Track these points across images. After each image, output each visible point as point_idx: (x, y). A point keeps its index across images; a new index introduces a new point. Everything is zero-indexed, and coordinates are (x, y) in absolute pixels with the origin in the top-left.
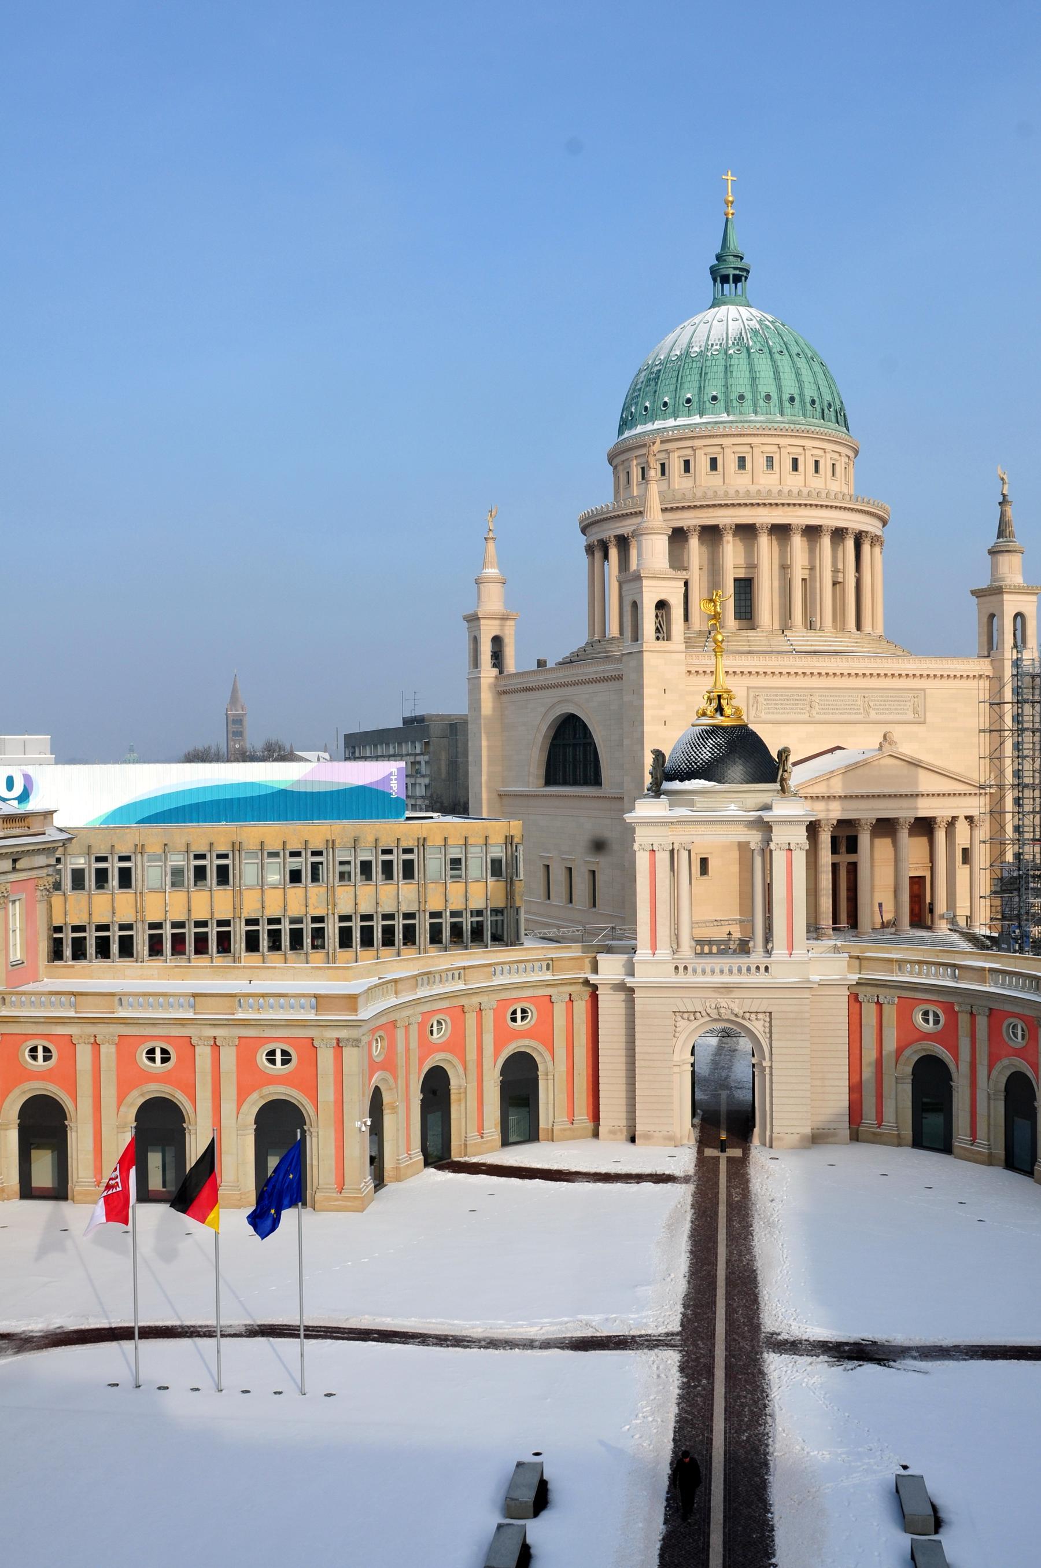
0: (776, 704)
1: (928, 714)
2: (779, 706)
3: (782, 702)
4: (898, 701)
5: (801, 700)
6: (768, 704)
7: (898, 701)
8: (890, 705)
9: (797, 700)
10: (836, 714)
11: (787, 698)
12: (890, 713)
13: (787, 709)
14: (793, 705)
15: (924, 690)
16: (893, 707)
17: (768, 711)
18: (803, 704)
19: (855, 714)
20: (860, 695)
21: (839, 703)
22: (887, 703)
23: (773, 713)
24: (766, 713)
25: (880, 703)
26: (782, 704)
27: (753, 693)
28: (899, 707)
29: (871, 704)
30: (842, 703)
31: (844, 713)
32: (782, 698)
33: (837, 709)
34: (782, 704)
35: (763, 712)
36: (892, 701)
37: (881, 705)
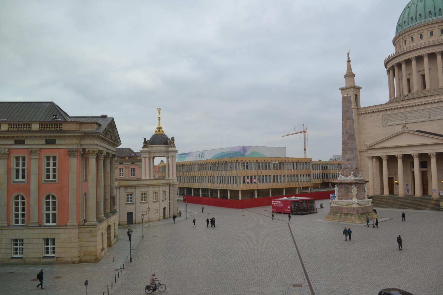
2: (394, 119)
5: (402, 116)
6: (390, 119)
13: (397, 120)
14: (399, 118)
18: (403, 118)
19: (424, 118)
20: (426, 111)
23: (392, 122)
25: (435, 112)
26: (395, 119)
27: (384, 117)
29: (431, 114)
32: (395, 117)
33: (417, 117)
35: (388, 122)
36: (440, 111)
37: (436, 113)
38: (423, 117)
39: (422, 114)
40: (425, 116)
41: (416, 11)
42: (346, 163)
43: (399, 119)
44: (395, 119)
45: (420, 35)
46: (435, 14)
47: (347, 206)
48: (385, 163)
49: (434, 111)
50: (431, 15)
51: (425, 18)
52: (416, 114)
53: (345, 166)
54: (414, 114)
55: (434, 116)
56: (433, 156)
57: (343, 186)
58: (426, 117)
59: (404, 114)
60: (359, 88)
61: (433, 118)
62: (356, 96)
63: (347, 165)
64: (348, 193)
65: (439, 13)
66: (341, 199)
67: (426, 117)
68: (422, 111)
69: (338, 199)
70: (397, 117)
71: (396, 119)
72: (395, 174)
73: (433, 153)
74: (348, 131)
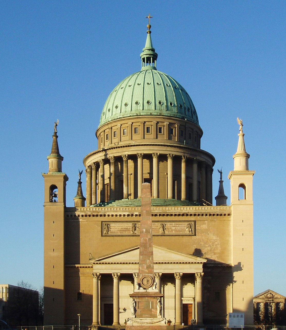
0: (115, 228)
3: (119, 227)
16: (177, 229)
28: (180, 229)
32: (119, 226)
39: (154, 227)
40: (158, 230)
43: (124, 229)
50: (162, 106)
58: (159, 231)
70: (122, 226)
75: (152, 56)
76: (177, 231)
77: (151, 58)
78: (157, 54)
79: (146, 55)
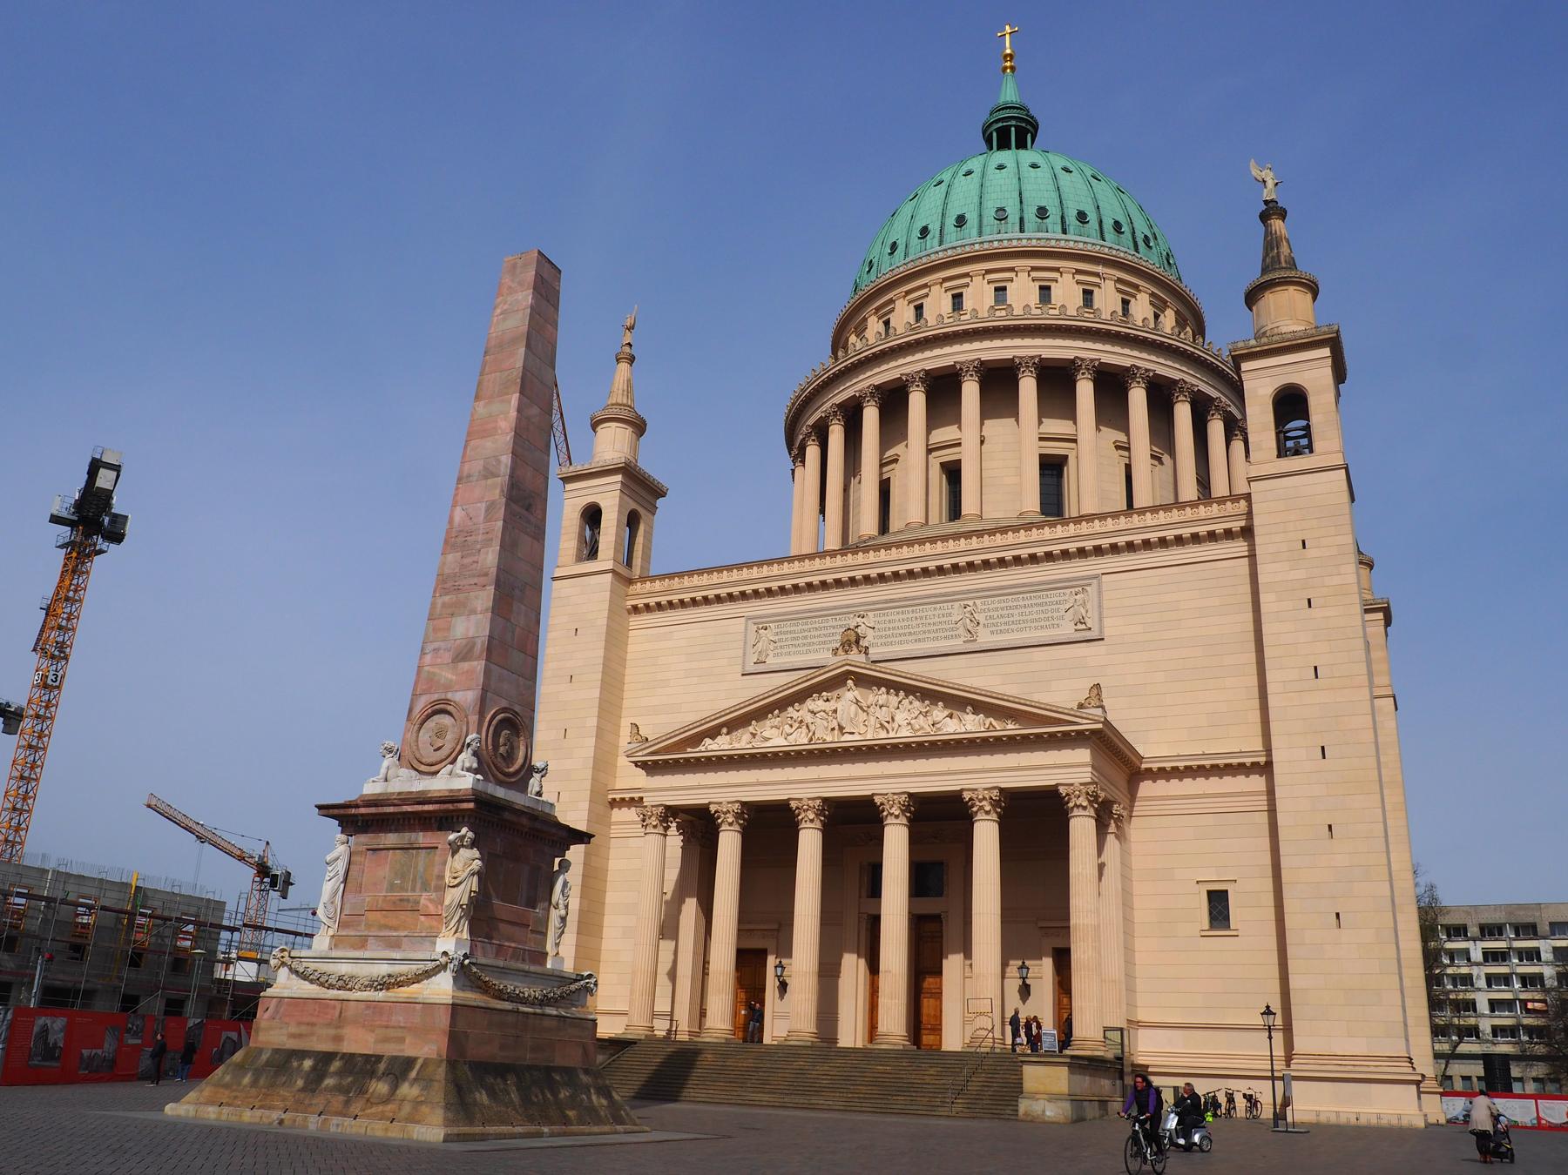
0: (794, 639)
1: (1107, 622)
2: (800, 641)
3: (806, 634)
4: (1041, 605)
6: (780, 640)
7: (1041, 605)
8: (1021, 614)
9: (834, 627)
10: (907, 642)
11: (813, 626)
12: (1021, 630)
15: (1096, 577)
17: (779, 651)
20: (956, 605)
21: (914, 623)
22: (1016, 612)
23: (789, 654)
24: (776, 655)
25: (1001, 612)
26: (806, 637)
28: (1042, 616)
29: (980, 617)
30: (919, 621)
31: (924, 640)
32: (805, 627)
34: (806, 637)
35: (771, 654)
38: (943, 635)
39: (937, 620)
41: (945, 204)
42: (447, 675)
44: (805, 641)
45: (954, 296)
46: (1022, 219)
47: (381, 995)
48: (729, 845)
49: (996, 605)
51: (980, 234)
52: (911, 615)
53: (436, 697)
54: (901, 616)
55: (992, 633)
56: (988, 808)
57: (391, 839)
58: (953, 633)
59: (852, 616)
60: (658, 492)
61: (985, 638)
62: (633, 521)
63: (448, 687)
64: (413, 890)
65: (1040, 221)
66: (362, 943)
67: (953, 633)
68: (938, 606)
69: (337, 941)
71: (809, 641)
72: (775, 927)
73: (985, 789)
74: (499, 462)
75: (1014, 123)
76: (1029, 625)
77: (1013, 129)
78: (1032, 118)
79: (997, 121)
